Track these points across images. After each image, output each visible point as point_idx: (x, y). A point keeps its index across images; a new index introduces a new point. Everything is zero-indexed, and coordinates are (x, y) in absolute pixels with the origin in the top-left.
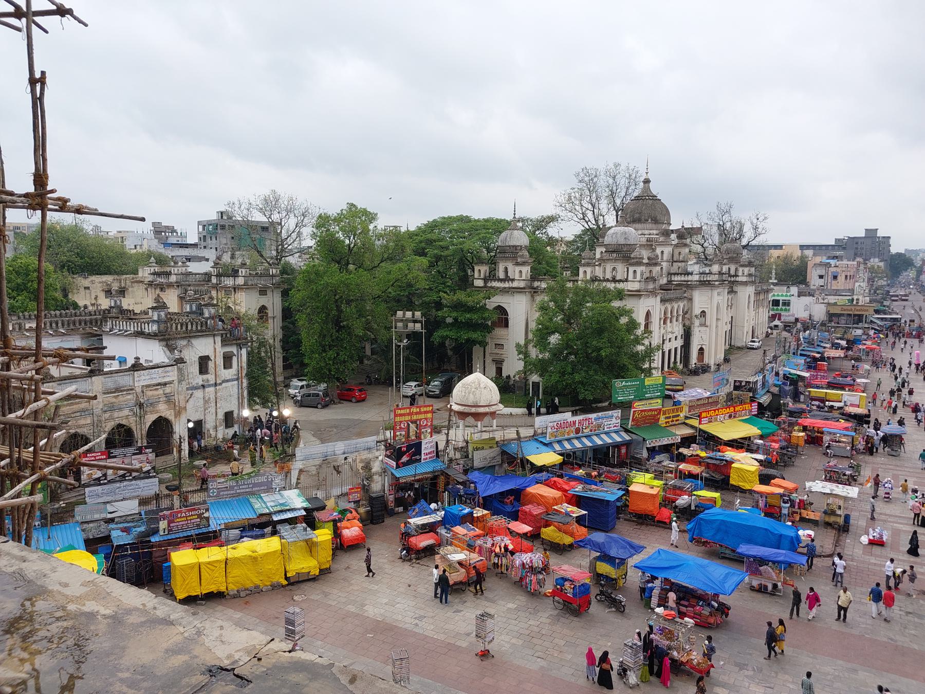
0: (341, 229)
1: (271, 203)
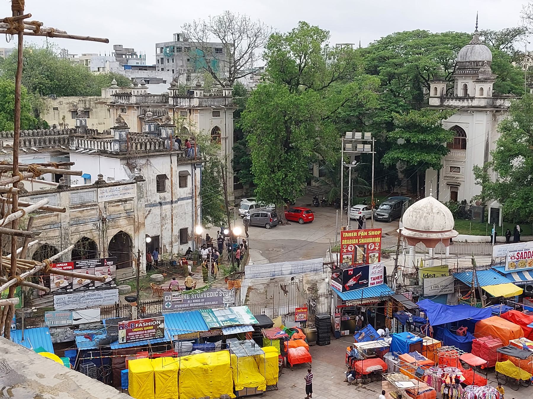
0: (292, 49)
1: (225, 25)
